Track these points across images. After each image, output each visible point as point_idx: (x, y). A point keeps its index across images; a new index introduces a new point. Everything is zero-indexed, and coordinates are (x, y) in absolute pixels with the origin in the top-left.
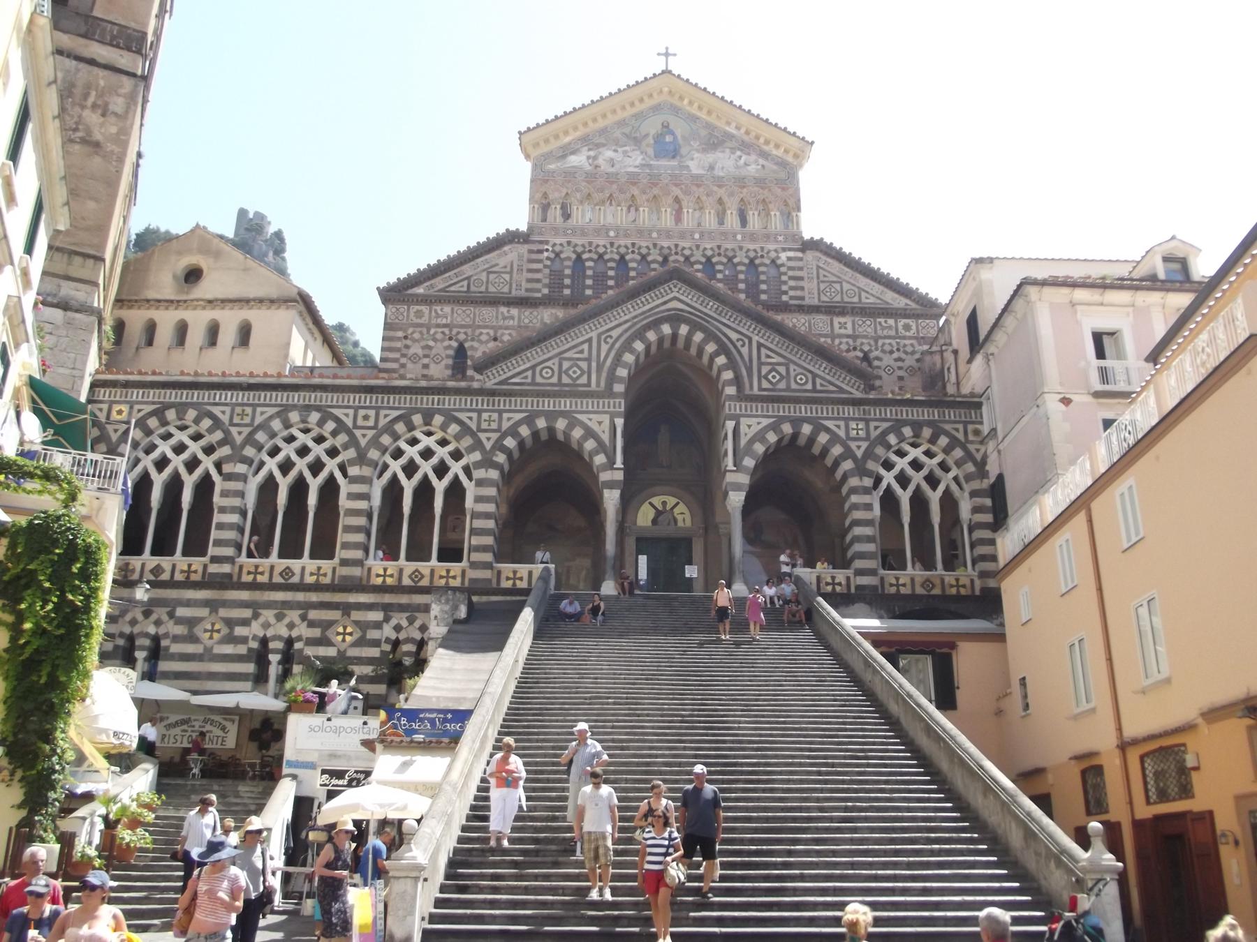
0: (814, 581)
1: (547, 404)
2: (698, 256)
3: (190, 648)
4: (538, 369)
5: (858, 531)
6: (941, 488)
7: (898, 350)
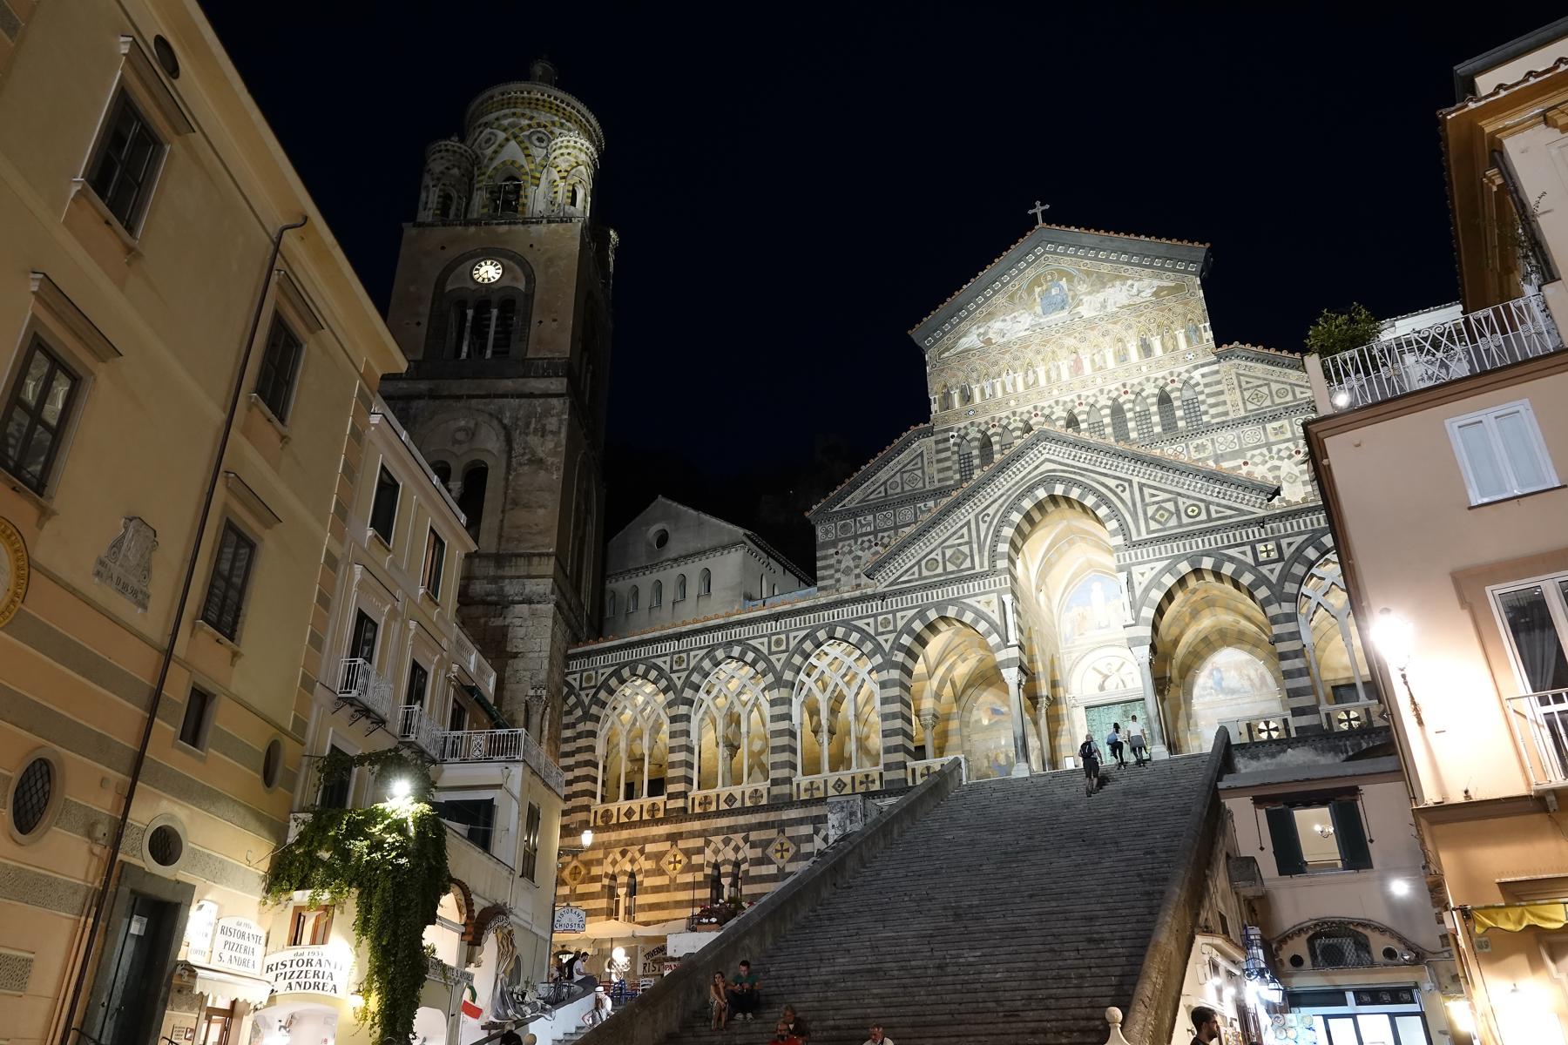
0: (1244, 730)
1: (937, 595)
2: (1104, 401)
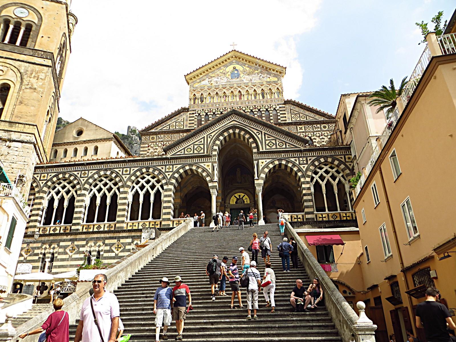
0: (290, 217)
1: (189, 161)
3: (64, 257)
4: (186, 149)
5: (305, 198)
6: (337, 180)
7: (322, 135)
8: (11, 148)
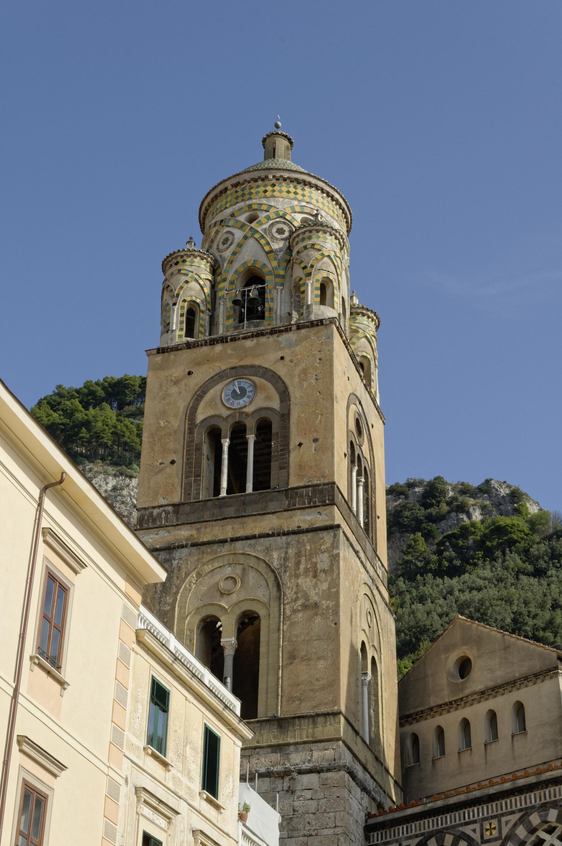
8: (298, 793)
